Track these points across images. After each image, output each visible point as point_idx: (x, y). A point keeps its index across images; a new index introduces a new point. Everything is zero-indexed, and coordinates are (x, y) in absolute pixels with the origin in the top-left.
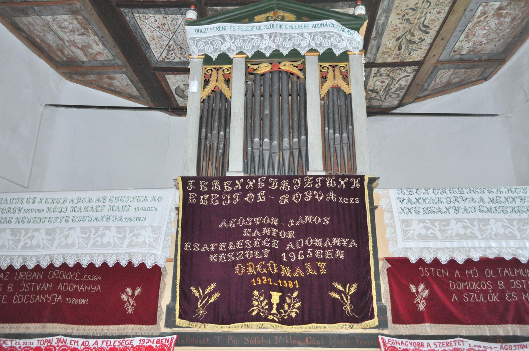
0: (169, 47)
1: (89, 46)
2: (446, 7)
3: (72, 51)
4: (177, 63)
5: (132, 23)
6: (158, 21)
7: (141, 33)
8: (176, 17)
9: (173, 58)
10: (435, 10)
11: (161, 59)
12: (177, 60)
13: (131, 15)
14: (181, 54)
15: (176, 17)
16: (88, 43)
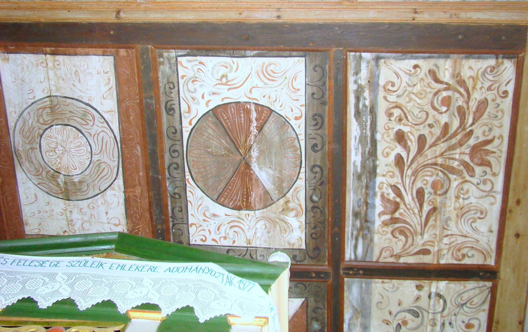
2: (479, 311)
10: (460, 318)
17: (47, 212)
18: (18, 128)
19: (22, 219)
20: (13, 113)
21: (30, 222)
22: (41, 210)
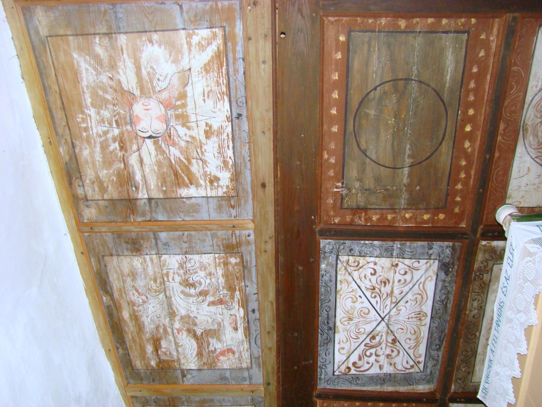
0: (373, 338)
1: (215, 333)
3: (176, 344)
4: (373, 379)
5: (326, 278)
6: (378, 275)
7: (332, 304)
8: (416, 265)
9: (367, 366)
11: (343, 368)
12: (375, 370)
13: (332, 259)
14: (388, 356)
15: (416, 265)
16: (219, 324)
17: (535, 184)
18: (534, 102)
19: (506, 193)
20: (534, 88)
21: (513, 195)
22: (528, 183)
